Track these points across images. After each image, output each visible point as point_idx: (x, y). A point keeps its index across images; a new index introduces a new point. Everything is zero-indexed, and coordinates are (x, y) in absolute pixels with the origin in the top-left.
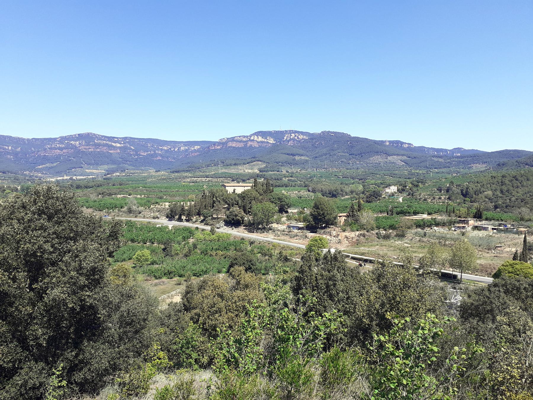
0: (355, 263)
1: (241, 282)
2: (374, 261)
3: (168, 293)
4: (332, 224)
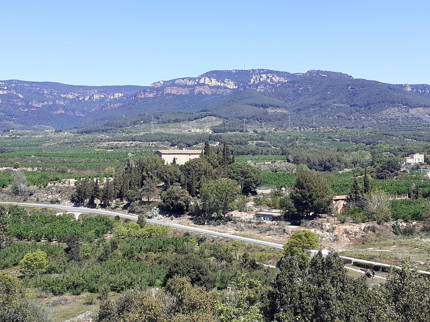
0: (360, 272)
1: (184, 301)
2: (389, 268)
3: (73, 317)
4: (324, 212)
